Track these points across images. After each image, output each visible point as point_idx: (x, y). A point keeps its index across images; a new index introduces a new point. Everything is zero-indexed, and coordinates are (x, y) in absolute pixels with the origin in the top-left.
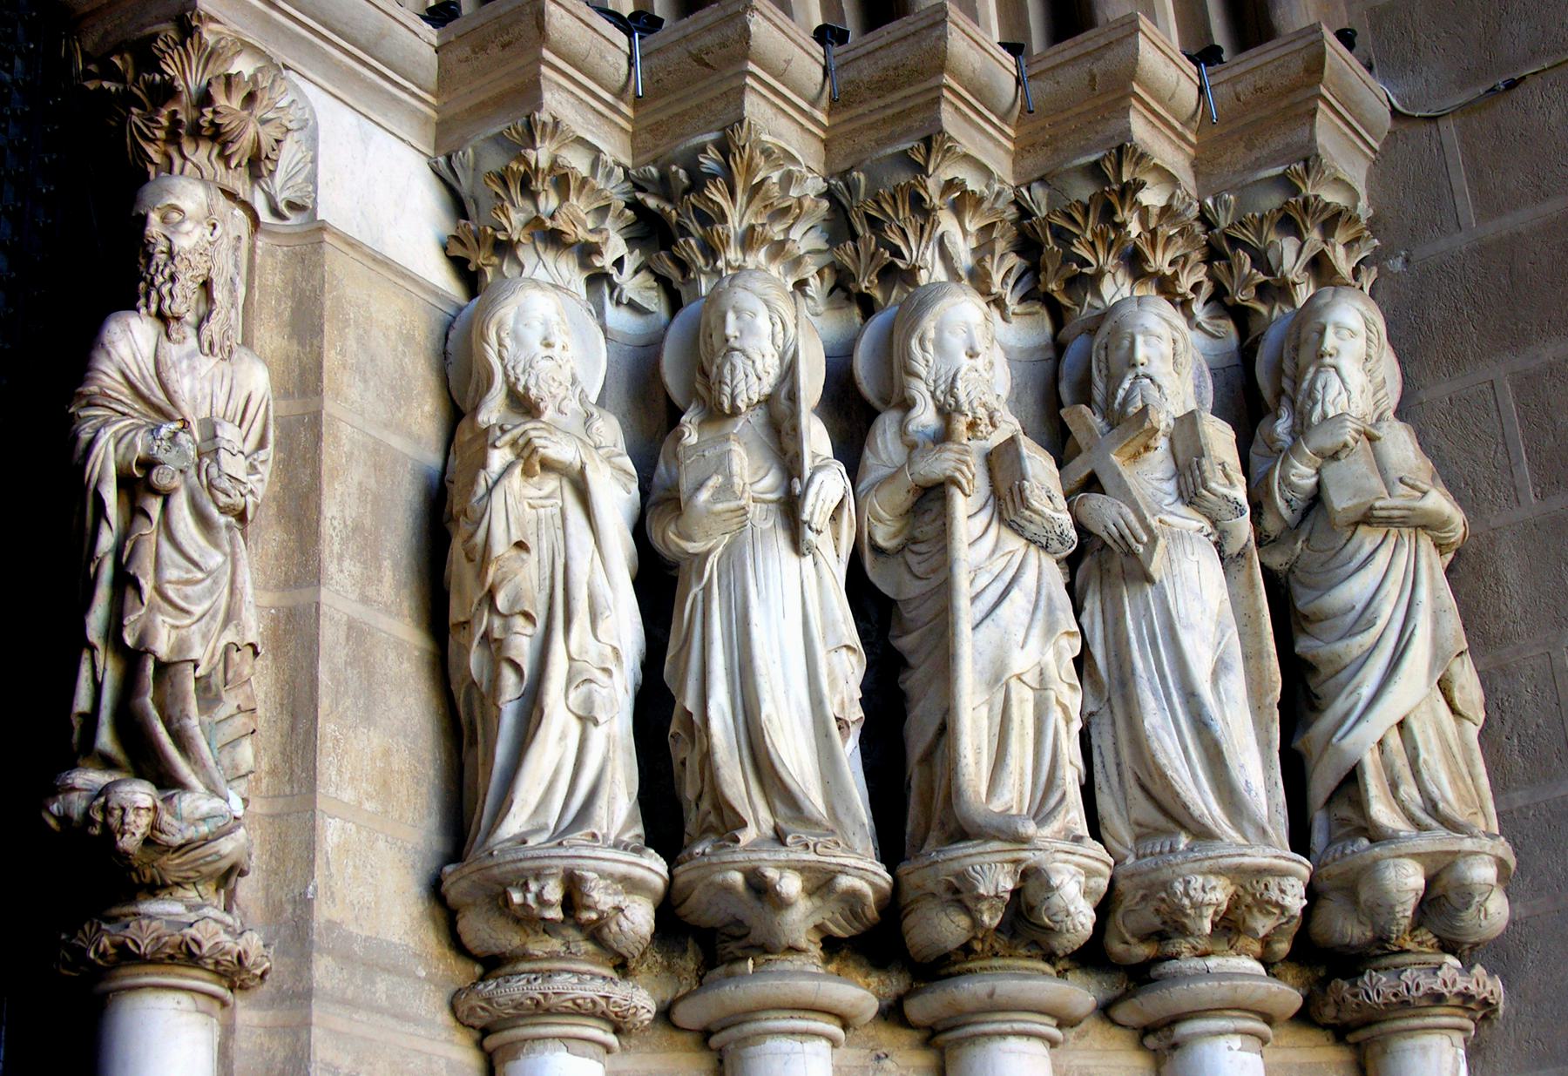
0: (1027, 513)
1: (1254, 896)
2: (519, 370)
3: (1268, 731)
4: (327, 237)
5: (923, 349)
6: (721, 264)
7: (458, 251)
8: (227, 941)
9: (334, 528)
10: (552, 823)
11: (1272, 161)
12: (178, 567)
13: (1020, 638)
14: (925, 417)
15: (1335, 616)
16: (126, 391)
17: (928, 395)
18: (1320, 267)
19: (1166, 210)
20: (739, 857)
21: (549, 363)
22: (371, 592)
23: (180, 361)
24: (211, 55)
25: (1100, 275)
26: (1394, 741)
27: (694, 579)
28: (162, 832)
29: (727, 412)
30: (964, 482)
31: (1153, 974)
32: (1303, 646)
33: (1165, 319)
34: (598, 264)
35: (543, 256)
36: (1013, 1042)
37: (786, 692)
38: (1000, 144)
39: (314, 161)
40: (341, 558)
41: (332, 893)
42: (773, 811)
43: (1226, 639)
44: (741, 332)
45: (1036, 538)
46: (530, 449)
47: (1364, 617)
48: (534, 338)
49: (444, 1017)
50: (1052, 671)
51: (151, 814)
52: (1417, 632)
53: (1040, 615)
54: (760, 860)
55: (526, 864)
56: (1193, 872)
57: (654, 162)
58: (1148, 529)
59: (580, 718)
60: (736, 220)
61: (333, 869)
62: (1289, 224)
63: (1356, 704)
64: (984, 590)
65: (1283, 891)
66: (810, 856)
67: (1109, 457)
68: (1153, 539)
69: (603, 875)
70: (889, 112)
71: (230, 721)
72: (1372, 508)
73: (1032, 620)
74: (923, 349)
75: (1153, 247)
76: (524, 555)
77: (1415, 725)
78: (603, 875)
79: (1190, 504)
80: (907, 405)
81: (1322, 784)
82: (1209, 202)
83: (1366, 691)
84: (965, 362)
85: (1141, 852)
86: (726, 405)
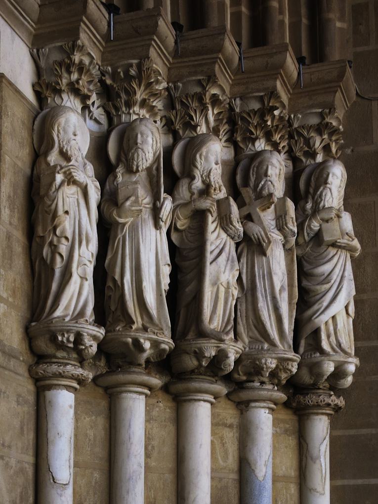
0: (231, 226)
1: (283, 366)
2: (64, 143)
3: (292, 312)
5: (201, 158)
6: (131, 111)
10: (71, 313)
11: (318, 106)
13: (223, 270)
14: (198, 184)
15: (317, 276)
17: (200, 176)
18: (327, 149)
19: (281, 118)
20: (132, 334)
21: (74, 142)
25: (257, 138)
26: (330, 322)
27: (119, 231)
29: (134, 171)
30: (212, 212)
31: (244, 386)
32: (305, 283)
33: (278, 161)
34: (88, 103)
36: (202, 403)
38: (228, 81)
42: (142, 319)
44: (142, 142)
46: (71, 176)
47: (327, 279)
48: (71, 131)
49: (26, 374)
50: (231, 282)
52: (344, 286)
53: (229, 262)
54: (139, 336)
55: (65, 328)
56: (268, 357)
57: (111, 66)
58: (268, 238)
59: (81, 277)
60: (140, 95)
62: (319, 129)
63: (322, 306)
65: (292, 366)
66: (155, 337)
67: (255, 209)
68: (270, 242)
69: (89, 334)
70: (196, 63)
72: (336, 242)
73: (227, 264)
74: (201, 158)
75: (276, 133)
76: (67, 216)
78: (89, 334)
79: (279, 230)
80: (193, 178)
81: (308, 330)
82: (292, 116)
83: (325, 304)
84: (214, 166)
85: (251, 347)
86: (135, 168)
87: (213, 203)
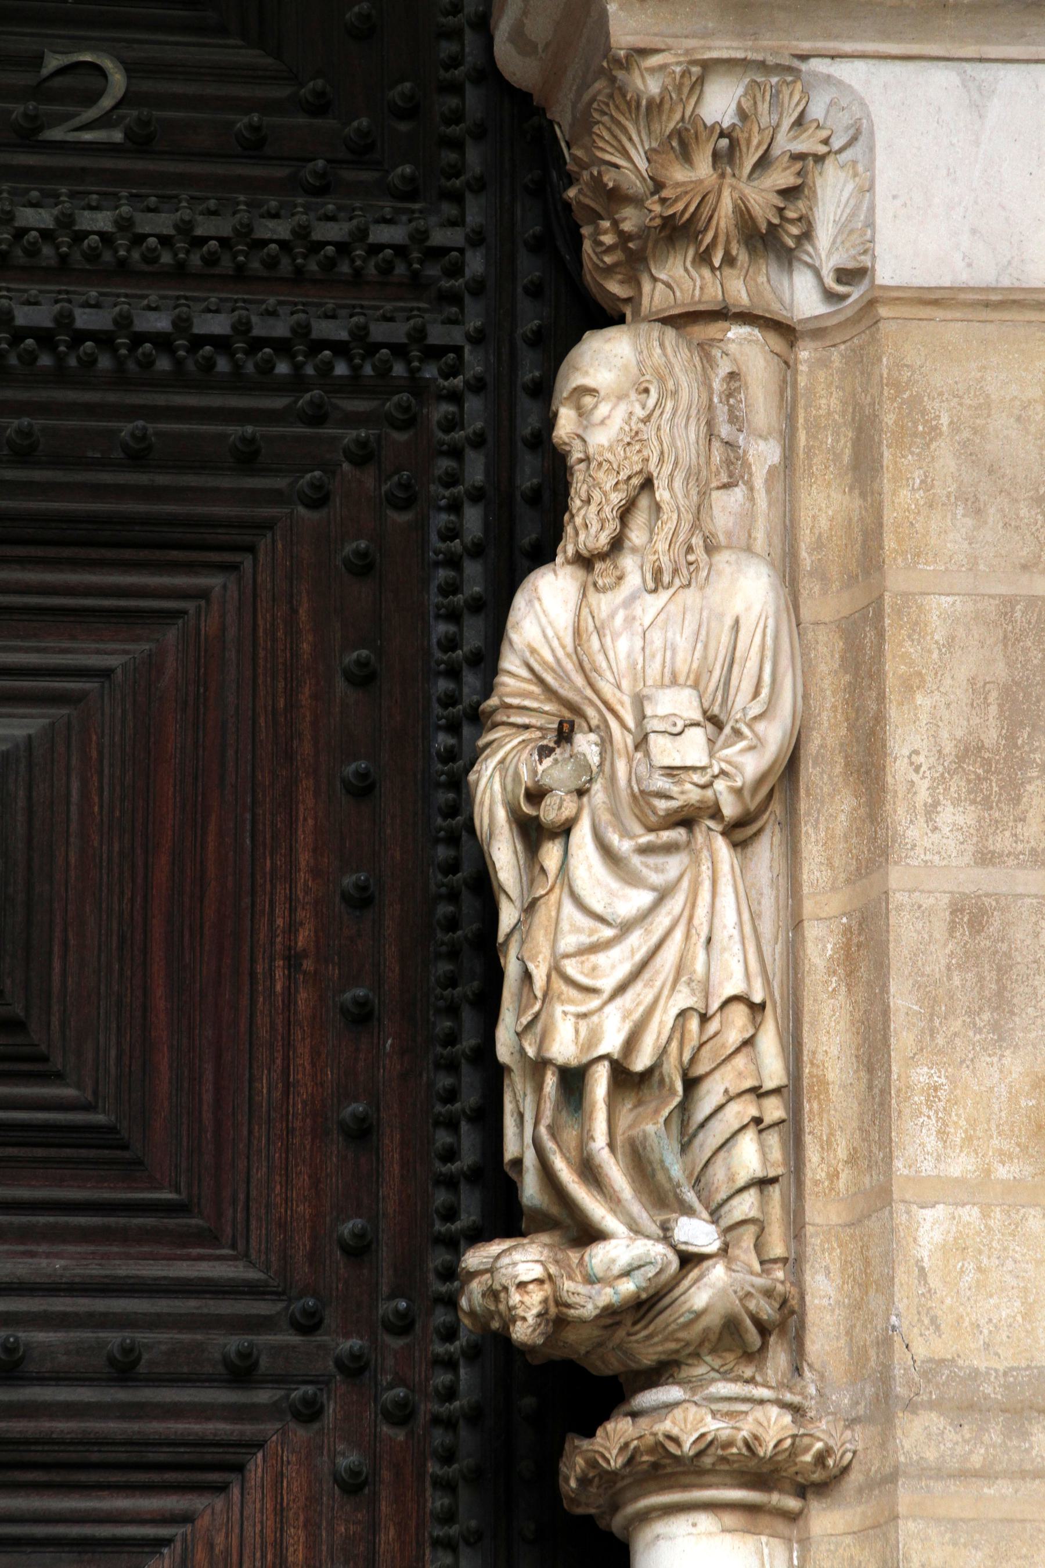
8: (713, 1426)
9: (917, 770)
12: (577, 930)
16: (536, 689)
22: (1002, 842)
23: (612, 616)
28: (569, 1306)
39: (871, 189)
40: (932, 809)
41: (934, 1320)
51: (547, 1286)
61: (934, 1282)
71: (720, 1116)
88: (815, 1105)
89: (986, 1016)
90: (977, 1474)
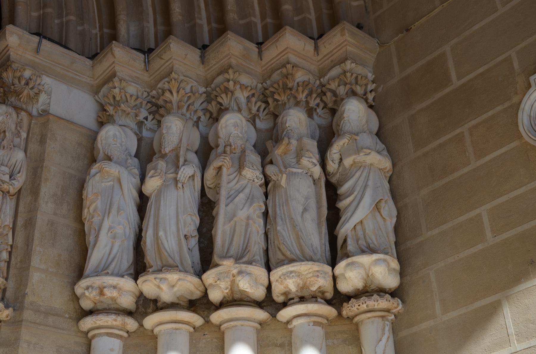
2: (106, 148)
4: (51, 117)
7: (100, 120)
13: (241, 207)
24: (15, 71)
30: (225, 164)
35: (121, 118)
37: (170, 229)
39: (50, 99)
40: (47, 202)
41: (34, 294)
43: (308, 202)
45: (250, 179)
53: (249, 200)
64: (232, 195)
75: (299, 94)
77: (365, 222)
81: (340, 242)
87: (225, 157)
88: (15, 250)
89: (51, 241)
90: (37, 324)
